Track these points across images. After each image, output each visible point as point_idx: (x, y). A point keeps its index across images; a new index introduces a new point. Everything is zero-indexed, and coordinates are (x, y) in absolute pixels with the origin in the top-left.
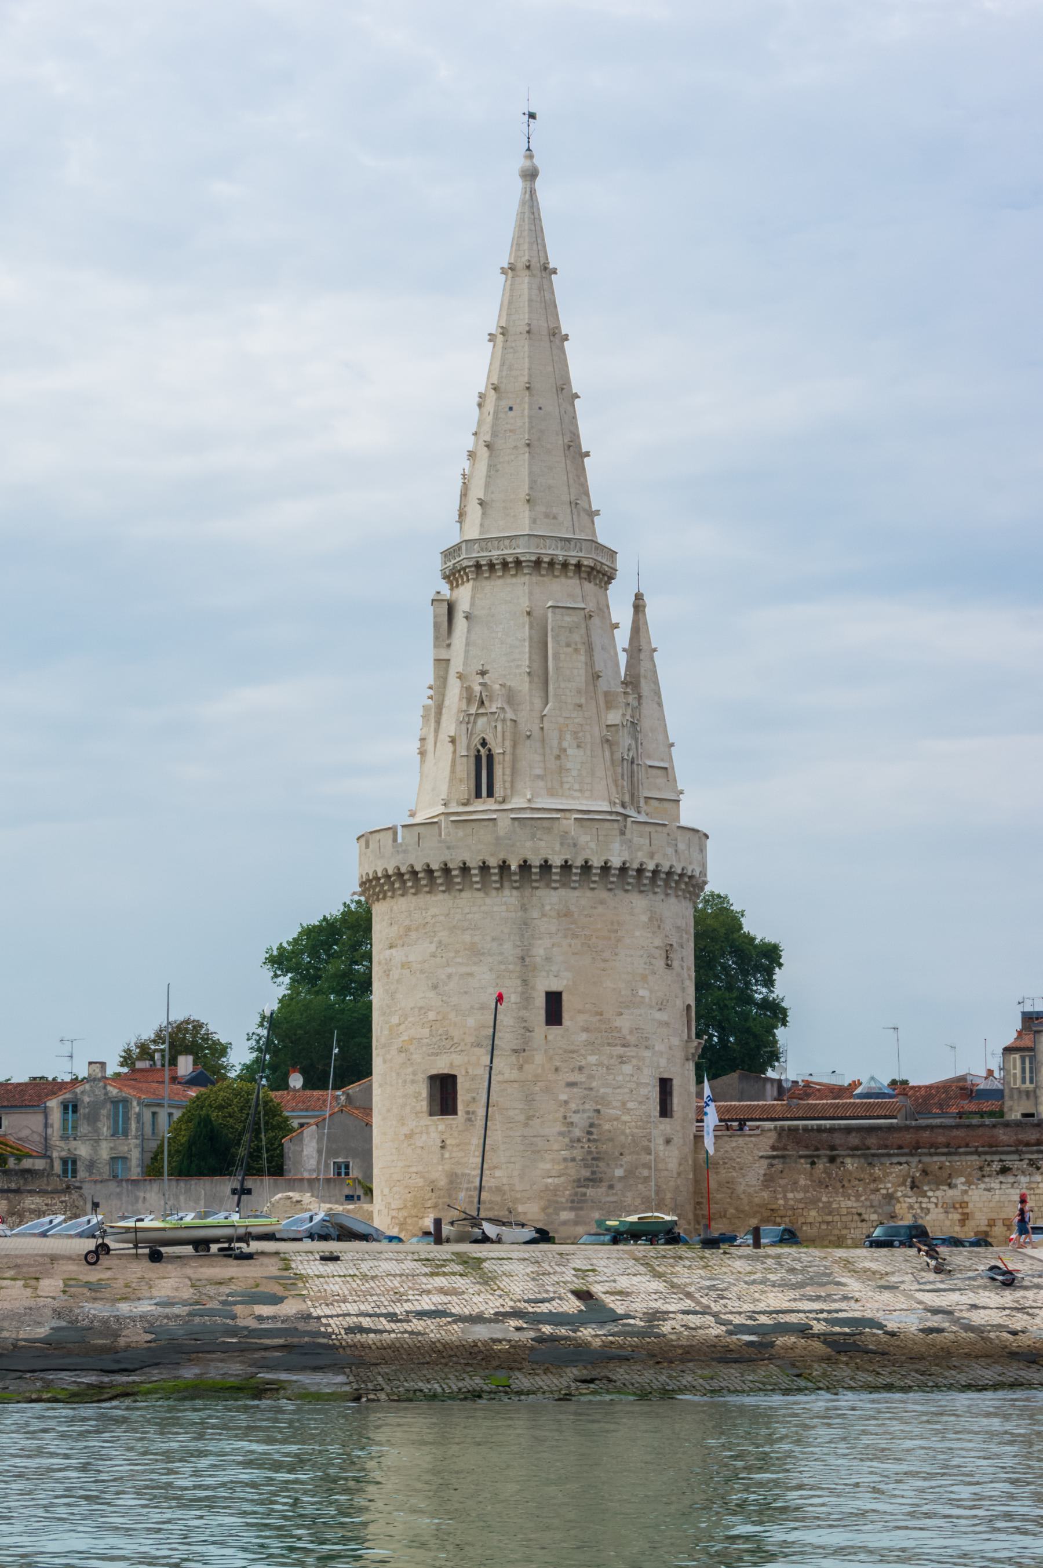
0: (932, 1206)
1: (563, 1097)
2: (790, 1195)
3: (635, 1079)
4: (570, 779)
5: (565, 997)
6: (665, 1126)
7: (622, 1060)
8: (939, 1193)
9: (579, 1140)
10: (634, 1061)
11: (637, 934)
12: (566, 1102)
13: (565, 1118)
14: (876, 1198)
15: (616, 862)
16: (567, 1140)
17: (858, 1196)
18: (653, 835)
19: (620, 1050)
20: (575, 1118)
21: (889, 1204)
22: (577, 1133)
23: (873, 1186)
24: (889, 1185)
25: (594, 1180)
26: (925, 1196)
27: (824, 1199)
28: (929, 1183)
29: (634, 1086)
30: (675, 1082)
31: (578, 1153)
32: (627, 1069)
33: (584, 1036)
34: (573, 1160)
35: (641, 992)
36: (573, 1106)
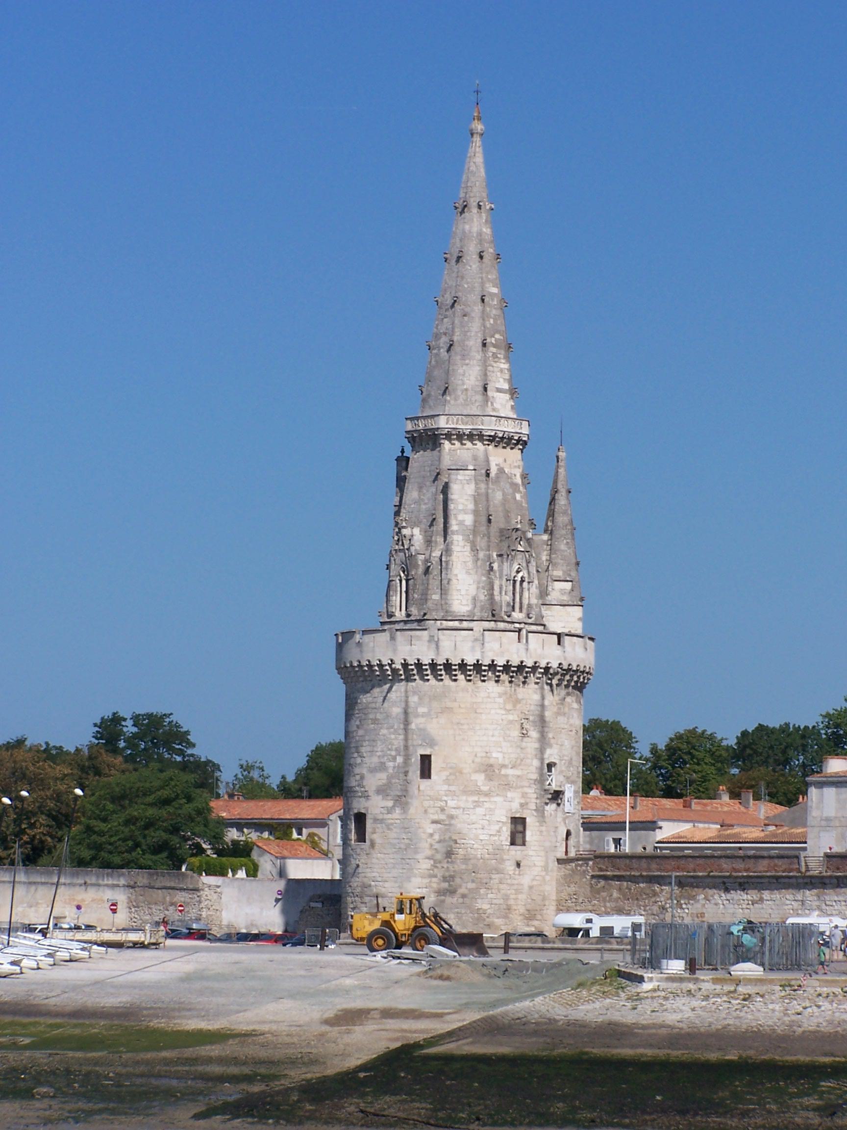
0: (685, 915)
1: (431, 831)
2: (608, 904)
3: (487, 818)
4: (460, 597)
5: (433, 757)
6: (516, 852)
7: (477, 805)
8: (689, 906)
9: (440, 862)
10: (487, 805)
11: (493, 712)
12: (431, 835)
13: (431, 845)
14: (655, 909)
15: (470, 660)
16: (432, 862)
17: (645, 906)
18: (504, 640)
19: (476, 798)
20: (437, 846)
21: (661, 913)
22: (439, 857)
23: (653, 899)
24: (662, 899)
25: (452, 892)
26: (682, 908)
27: (627, 908)
28: (685, 898)
30: (528, 820)
31: (440, 873)
32: (480, 811)
33: (446, 787)
34: (436, 876)
35: (494, 755)
36: (437, 837)
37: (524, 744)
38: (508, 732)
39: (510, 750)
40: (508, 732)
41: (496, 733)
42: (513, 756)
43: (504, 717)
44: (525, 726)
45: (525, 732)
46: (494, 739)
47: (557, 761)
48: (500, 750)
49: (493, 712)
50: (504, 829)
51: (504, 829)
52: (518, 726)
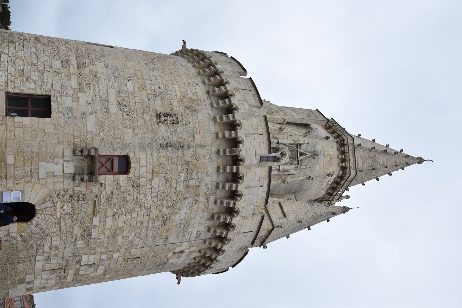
10: (64, 71)
29: (41, 66)
30: (47, 119)
37: (147, 117)
38: (158, 99)
39: (138, 99)
40: (158, 99)
41: (156, 88)
42: (132, 102)
43: (175, 98)
44: (169, 119)
45: (163, 119)
46: (148, 85)
47: (131, 175)
48: (136, 89)
49: (176, 87)
50: (32, 86)
51: (32, 86)
52: (168, 111)
